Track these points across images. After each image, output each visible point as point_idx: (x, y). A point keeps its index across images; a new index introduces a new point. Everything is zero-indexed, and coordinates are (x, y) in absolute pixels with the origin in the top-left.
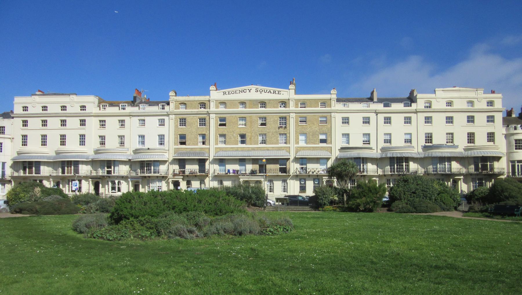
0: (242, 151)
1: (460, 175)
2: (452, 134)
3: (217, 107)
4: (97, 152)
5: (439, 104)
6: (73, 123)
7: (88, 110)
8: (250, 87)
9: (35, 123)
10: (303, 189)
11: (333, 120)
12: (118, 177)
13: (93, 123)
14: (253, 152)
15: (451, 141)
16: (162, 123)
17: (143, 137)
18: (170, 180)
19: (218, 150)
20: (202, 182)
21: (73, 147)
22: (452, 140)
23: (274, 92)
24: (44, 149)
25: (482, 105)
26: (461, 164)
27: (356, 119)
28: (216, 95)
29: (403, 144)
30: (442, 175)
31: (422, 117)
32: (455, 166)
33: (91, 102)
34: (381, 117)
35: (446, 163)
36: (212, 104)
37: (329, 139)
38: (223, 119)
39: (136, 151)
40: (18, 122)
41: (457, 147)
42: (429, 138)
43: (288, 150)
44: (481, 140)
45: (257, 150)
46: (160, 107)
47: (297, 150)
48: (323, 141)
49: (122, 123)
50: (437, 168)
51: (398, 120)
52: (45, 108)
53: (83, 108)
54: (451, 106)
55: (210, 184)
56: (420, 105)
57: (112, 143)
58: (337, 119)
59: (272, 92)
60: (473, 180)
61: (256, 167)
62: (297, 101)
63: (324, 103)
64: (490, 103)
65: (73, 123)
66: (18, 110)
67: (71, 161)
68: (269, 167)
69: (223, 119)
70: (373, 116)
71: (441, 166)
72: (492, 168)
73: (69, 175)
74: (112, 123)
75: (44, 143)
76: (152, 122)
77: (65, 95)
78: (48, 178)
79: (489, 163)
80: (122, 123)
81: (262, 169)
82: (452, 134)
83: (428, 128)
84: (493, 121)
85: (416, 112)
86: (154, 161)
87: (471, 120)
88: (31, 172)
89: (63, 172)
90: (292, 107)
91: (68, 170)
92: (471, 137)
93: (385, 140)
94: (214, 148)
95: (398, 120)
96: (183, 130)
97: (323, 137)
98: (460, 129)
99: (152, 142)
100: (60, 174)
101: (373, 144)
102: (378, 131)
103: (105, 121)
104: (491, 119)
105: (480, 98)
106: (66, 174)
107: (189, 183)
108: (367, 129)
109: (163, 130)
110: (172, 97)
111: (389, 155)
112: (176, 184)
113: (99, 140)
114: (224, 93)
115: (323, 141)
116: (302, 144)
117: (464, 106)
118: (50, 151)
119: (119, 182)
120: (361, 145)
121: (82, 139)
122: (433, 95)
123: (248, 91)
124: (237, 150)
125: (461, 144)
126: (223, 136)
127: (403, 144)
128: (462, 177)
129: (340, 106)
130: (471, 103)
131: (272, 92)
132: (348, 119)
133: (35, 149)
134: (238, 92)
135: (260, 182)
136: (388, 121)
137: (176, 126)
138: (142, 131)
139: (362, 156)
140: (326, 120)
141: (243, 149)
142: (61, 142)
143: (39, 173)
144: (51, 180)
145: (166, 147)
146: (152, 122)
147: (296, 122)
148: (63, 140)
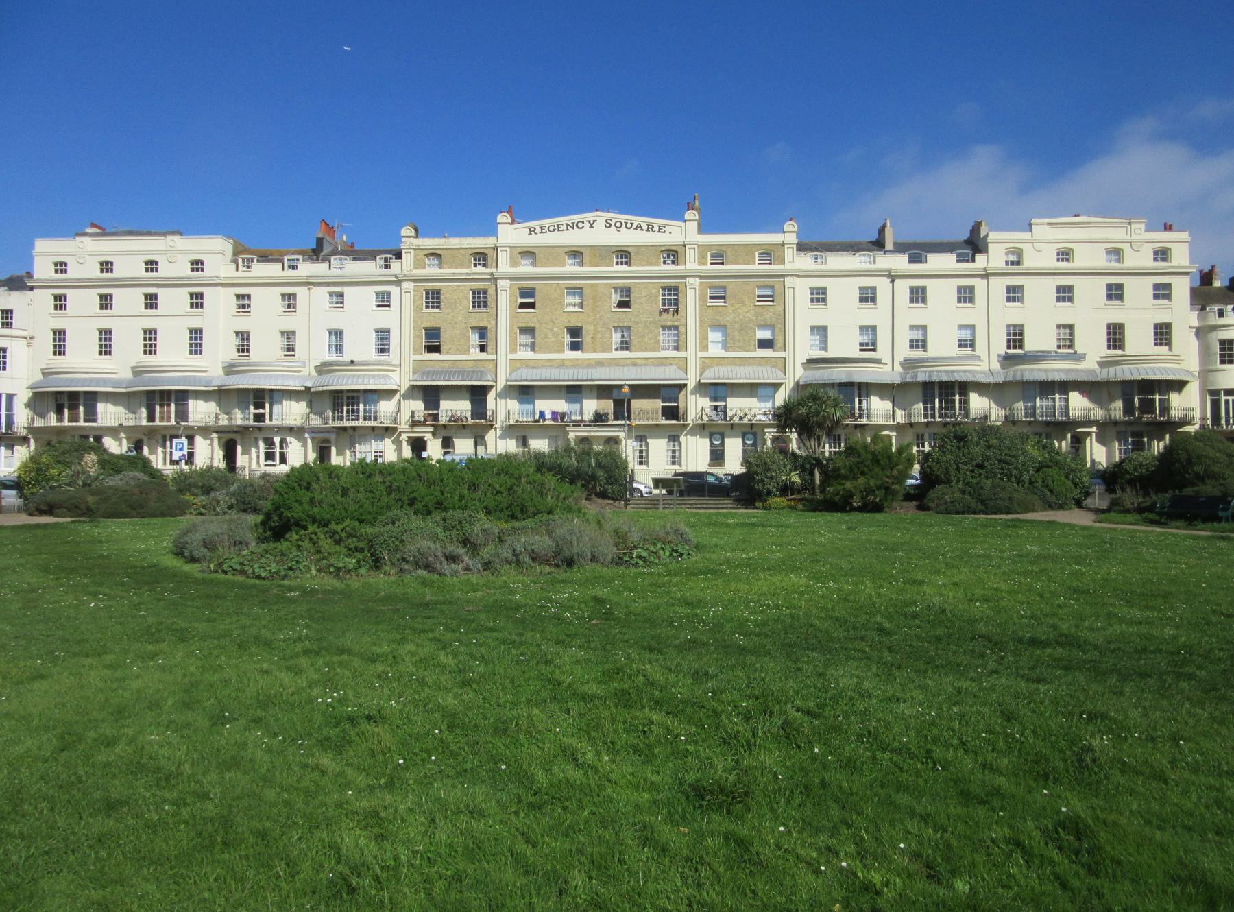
0: (574, 366)
1: (1089, 423)
2: (1071, 327)
3: (514, 263)
4: (230, 370)
5: (1039, 256)
6: (174, 300)
7: (209, 271)
8: (591, 216)
9: (83, 301)
10: (717, 457)
11: (789, 292)
12: (280, 430)
13: (220, 302)
14: (599, 369)
15: (1068, 343)
16: (384, 301)
17: (338, 334)
18: (404, 437)
19: (515, 364)
20: (479, 440)
21: (173, 361)
22: (1071, 341)
23: (650, 228)
24: (105, 363)
25: (1142, 258)
26: (1091, 399)
27: (844, 293)
28: (511, 234)
29: (954, 351)
30: (1048, 424)
31: (999, 286)
32: (1078, 404)
33: (215, 250)
34: (903, 286)
35: (1057, 396)
36: (503, 257)
37: (779, 339)
38: (527, 293)
39: (323, 369)
40: (45, 298)
41: (1082, 357)
42: (1016, 336)
43: (683, 364)
44: (1139, 341)
45: (609, 365)
46: (380, 262)
47: (705, 365)
48: (765, 344)
49: (290, 301)
50: (1034, 408)
51: (942, 293)
52: (107, 266)
53: (197, 265)
54: (1067, 260)
55: (499, 445)
56: (994, 257)
57: (265, 349)
58: (799, 290)
59: (645, 227)
60: (1121, 437)
61: (608, 405)
62: (703, 248)
63: (768, 254)
64: (1162, 254)
65: (174, 300)
66: (43, 270)
67: (169, 392)
68: (636, 404)
69: (527, 293)
70: (883, 285)
71: (1045, 403)
72: (1165, 409)
73: (165, 424)
74: (266, 301)
75: (105, 348)
76: (361, 299)
77: (155, 234)
78: (114, 432)
79: (1157, 397)
80: (290, 301)
81: (622, 409)
82: (1071, 327)
83: (1015, 314)
84: (1168, 297)
85: (986, 275)
86: (366, 391)
87: (1115, 293)
88: (74, 418)
89: (151, 418)
90: (691, 263)
91: (161, 413)
92: (1116, 335)
93: (911, 341)
94: (507, 361)
95: (942, 293)
96: (434, 317)
97: (765, 334)
98: (1091, 315)
99: (361, 347)
100: (144, 423)
101: (883, 352)
102: (895, 319)
103: (249, 297)
104: (1163, 292)
105: (1138, 245)
106: (157, 423)
107: (447, 444)
108: (869, 315)
109: (386, 319)
110: (408, 239)
111: (922, 377)
112: (418, 445)
113: (235, 341)
114: (532, 231)
115: (765, 344)
116: (715, 350)
117: (1100, 260)
118: (119, 367)
119: (282, 442)
120: (854, 353)
121: (196, 340)
122: (1026, 236)
123: (587, 225)
124: (562, 364)
125: (1092, 354)
126: (528, 331)
127: (954, 351)
128: (1094, 429)
129: (805, 262)
130: (1116, 253)
131: (645, 227)
132: (824, 290)
133: (83, 364)
134: (564, 227)
135: (616, 441)
136: (918, 295)
137: (417, 309)
138: (337, 320)
139: (857, 379)
140: (772, 293)
141: (575, 363)
142: (145, 346)
143: (95, 421)
144: (122, 435)
145: (393, 357)
146: (361, 299)
147: (702, 299)
148: (150, 341)
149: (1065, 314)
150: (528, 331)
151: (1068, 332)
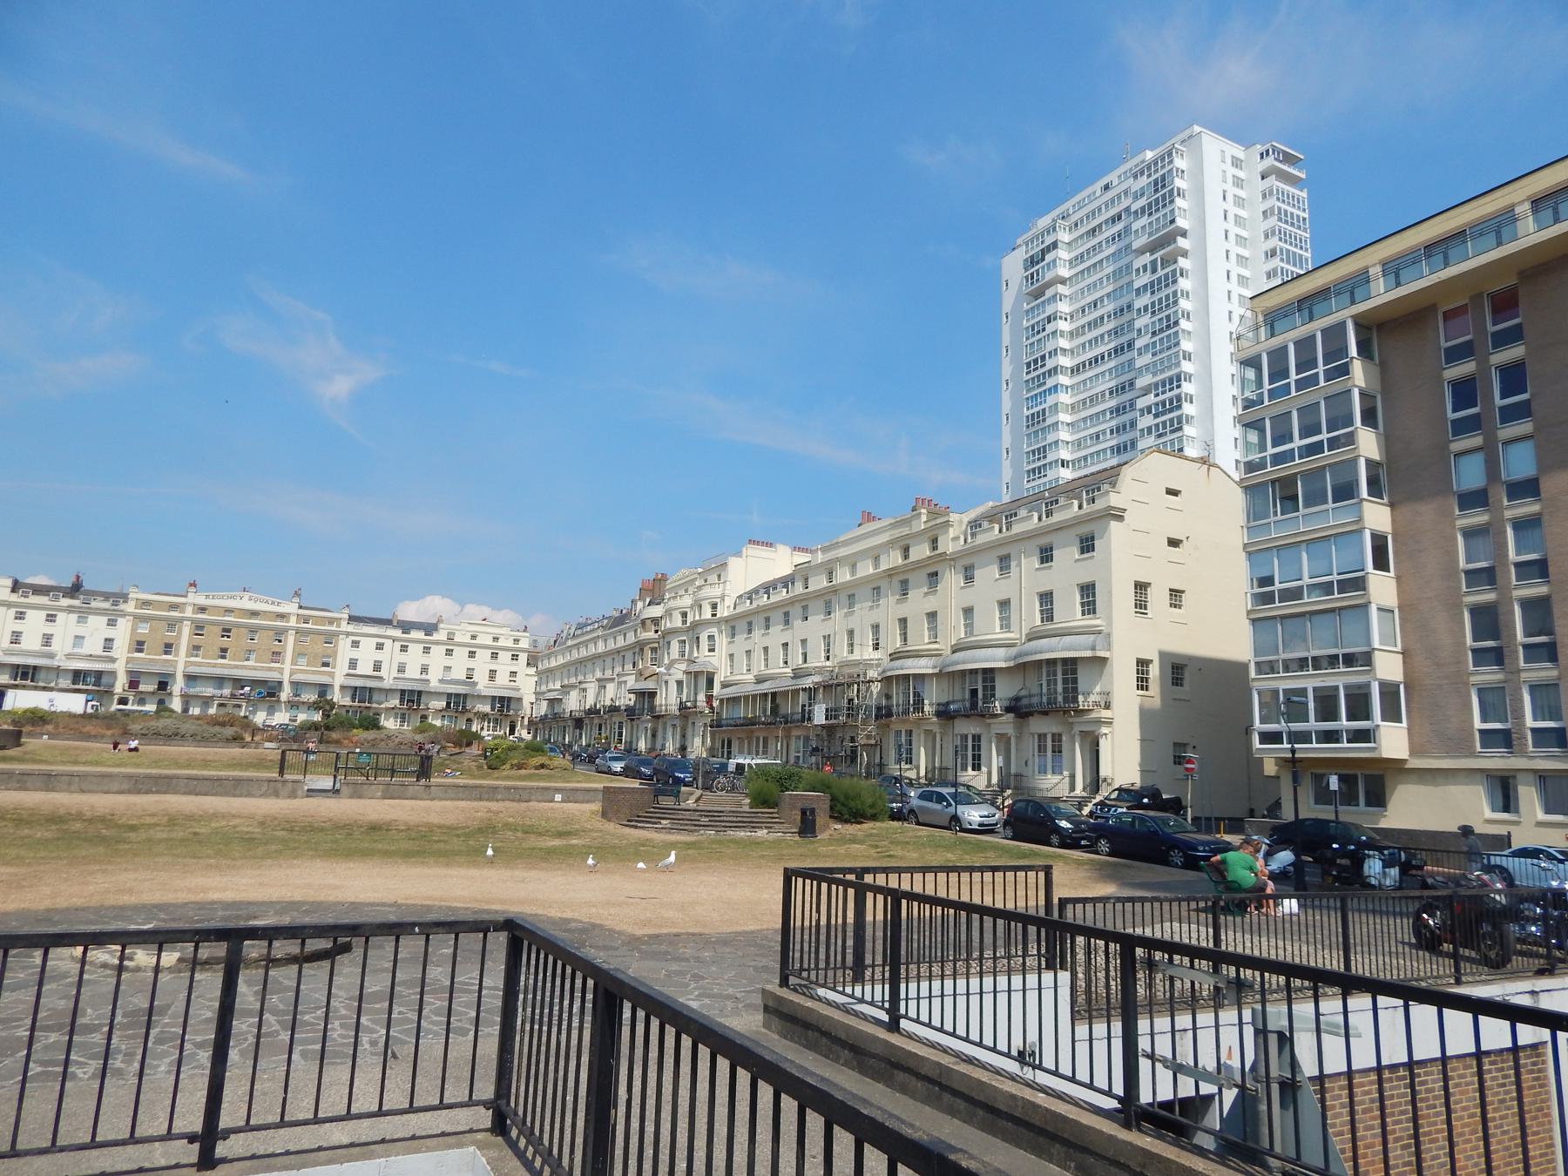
27: (368, 645)
34: (398, 645)
41: (475, 684)
43: (281, 671)
56: (440, 636)
63: (331, 621)
64: (516, 641)
80: (51, 618)
85: (437, 643)
90: (293, 622)
92: (493, 674)
94: (181, 662)
95: (415, 650)
101: (384, 673)
104: (515, 657)
108: (379, 656)
120: (371, 673)
124: (215, 666)
136: (404, 649)
141: (223, 666)
149: (471, 663)
150: (197, 648)
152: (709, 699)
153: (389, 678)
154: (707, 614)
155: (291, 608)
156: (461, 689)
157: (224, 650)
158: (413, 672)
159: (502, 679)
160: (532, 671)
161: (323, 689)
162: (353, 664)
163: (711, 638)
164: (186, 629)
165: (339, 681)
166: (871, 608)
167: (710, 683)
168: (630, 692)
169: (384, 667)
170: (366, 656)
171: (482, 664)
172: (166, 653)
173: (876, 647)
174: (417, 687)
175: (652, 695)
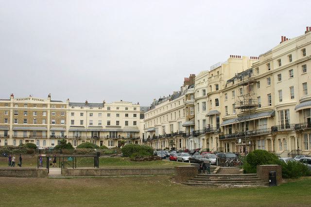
31: (106, 114)
36: (12, 105)
41: (120, 127)
42: (109, 123)
47: (51, 127)
51: (95, 114)
56: (105, 108)
58: (69, 115)
64: (135, 109)
83: (109, 119)
90: (49, 108)
92: (127, 123)
101: (84, 125)
104: (135, 115)
120: (79, 125)
124: (23, 126)
127: (98, 125)
129: (70, 108)
135: (33, 141)
136: (91, 115)
147: (51, 114)
151: (118, 122)
152: (218, 125)
153: (86, 125)
154: (214, 89)
155: (47, 102)
156: (115, 130)
157: (25, 120)
158: (96, 124)
159: (131, 124)
160: (142, 120)
161: (62, 132)
162: (73, 122)
163: (217, 100)
164: (11, 113)
165: (68, 128)
166: (259, 87)
167: (218, 120)
168: (183, 126)
169: (84, 123)
170: (77, 119)
171: (122, 120)
172: (6, 122)
173: (292, 97)
174: (98, 129)
175: (193, 126)
